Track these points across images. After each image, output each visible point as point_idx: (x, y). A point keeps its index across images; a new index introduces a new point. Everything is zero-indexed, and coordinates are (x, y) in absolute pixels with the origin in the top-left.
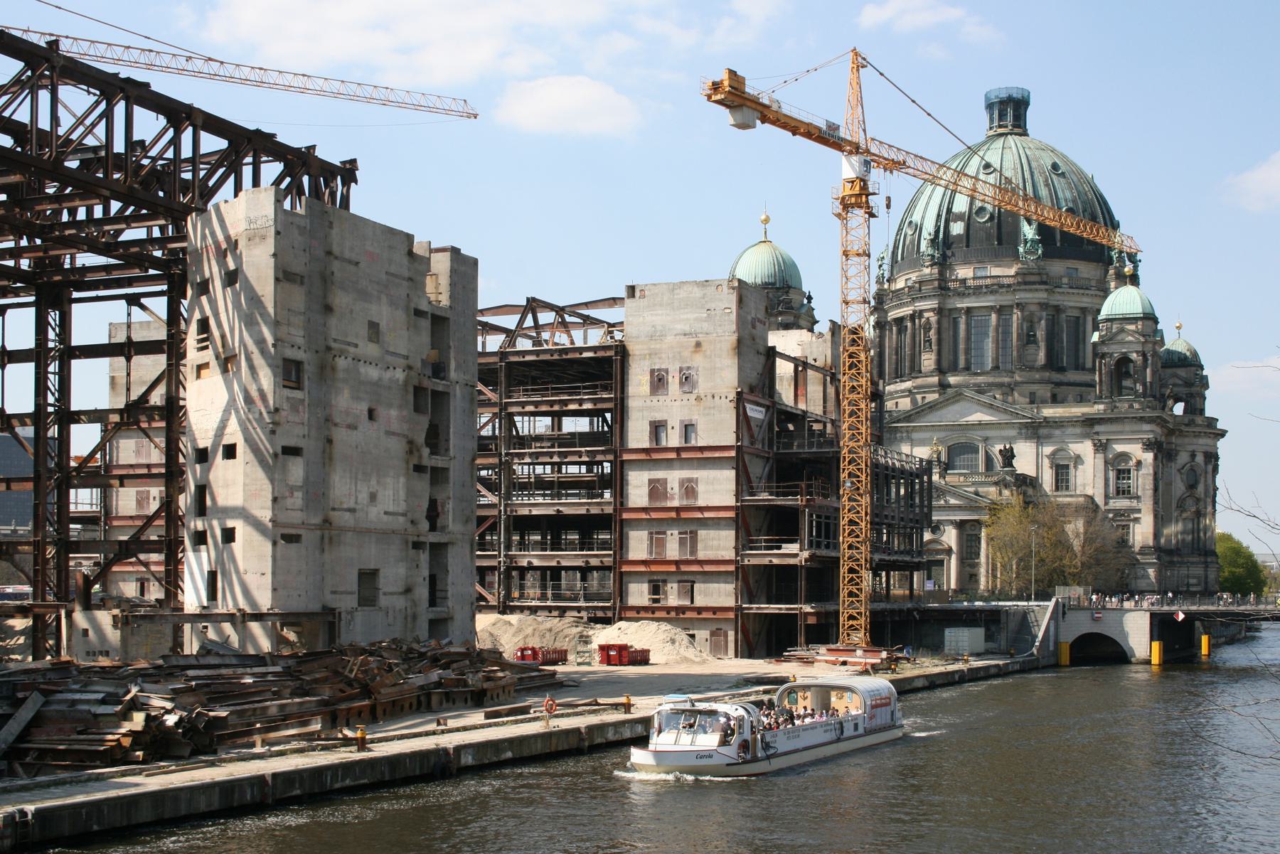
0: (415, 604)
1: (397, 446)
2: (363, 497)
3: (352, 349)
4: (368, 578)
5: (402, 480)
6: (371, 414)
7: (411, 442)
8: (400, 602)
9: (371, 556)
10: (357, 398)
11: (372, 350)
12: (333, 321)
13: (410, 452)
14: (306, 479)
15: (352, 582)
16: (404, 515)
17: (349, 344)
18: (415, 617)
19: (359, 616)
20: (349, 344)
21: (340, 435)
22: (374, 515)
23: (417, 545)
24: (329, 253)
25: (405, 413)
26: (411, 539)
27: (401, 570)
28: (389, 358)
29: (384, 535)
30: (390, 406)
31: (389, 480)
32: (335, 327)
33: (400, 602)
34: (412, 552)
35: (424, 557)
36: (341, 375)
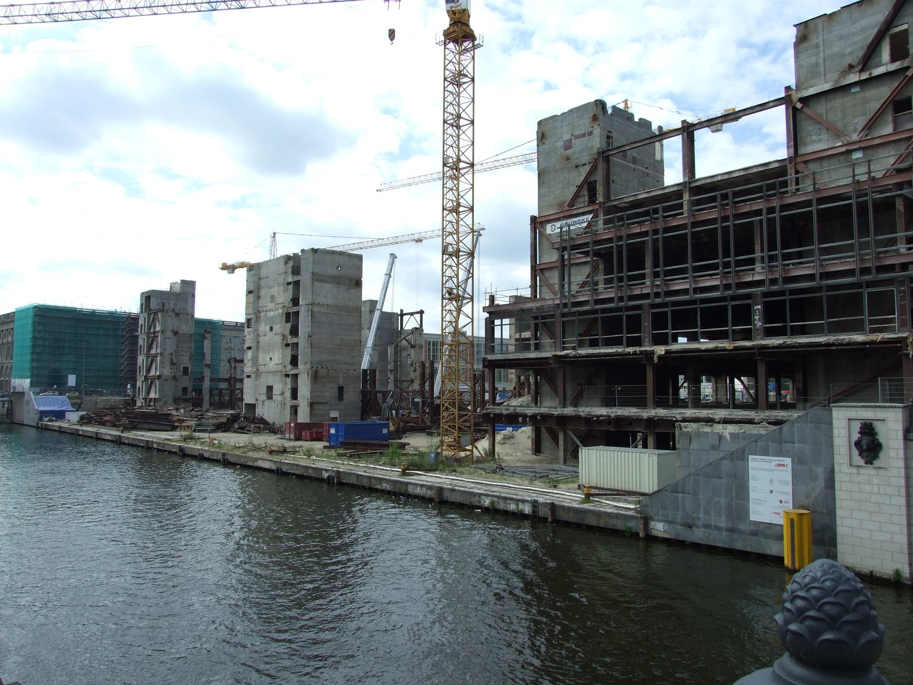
0: (285, 399)
1: (279, 339)
2: (268, 359)
3: (265, 308)
4: (270, 389)
5: (280, 351)
6: (271, 329)
7: (284, 336)
8: (279, 398)
9: (270, 380)
10: (266, 325)
11: (271, 306)
12: (260, 300)
13: (283, 339)
14: (252, 357)
15: (264, 390)
16: (281, 364)
17: (265, 306)
18: (285, 404)
19: (266, 403)
20: (265, 306)
21: (262, 339)
22: (272, 366)
23: (287, 376)
24: (260, 279)
25: (282, 325)
26: (284, 373)
27: (280, 386)
28: (277, 306)
29: (274, 373)
30: (277, 324)
31: (276, 352)
32: (262, 303)
33: (279, 398)
34: (284, 378)
35: (289, 380)
36: (262, 318)
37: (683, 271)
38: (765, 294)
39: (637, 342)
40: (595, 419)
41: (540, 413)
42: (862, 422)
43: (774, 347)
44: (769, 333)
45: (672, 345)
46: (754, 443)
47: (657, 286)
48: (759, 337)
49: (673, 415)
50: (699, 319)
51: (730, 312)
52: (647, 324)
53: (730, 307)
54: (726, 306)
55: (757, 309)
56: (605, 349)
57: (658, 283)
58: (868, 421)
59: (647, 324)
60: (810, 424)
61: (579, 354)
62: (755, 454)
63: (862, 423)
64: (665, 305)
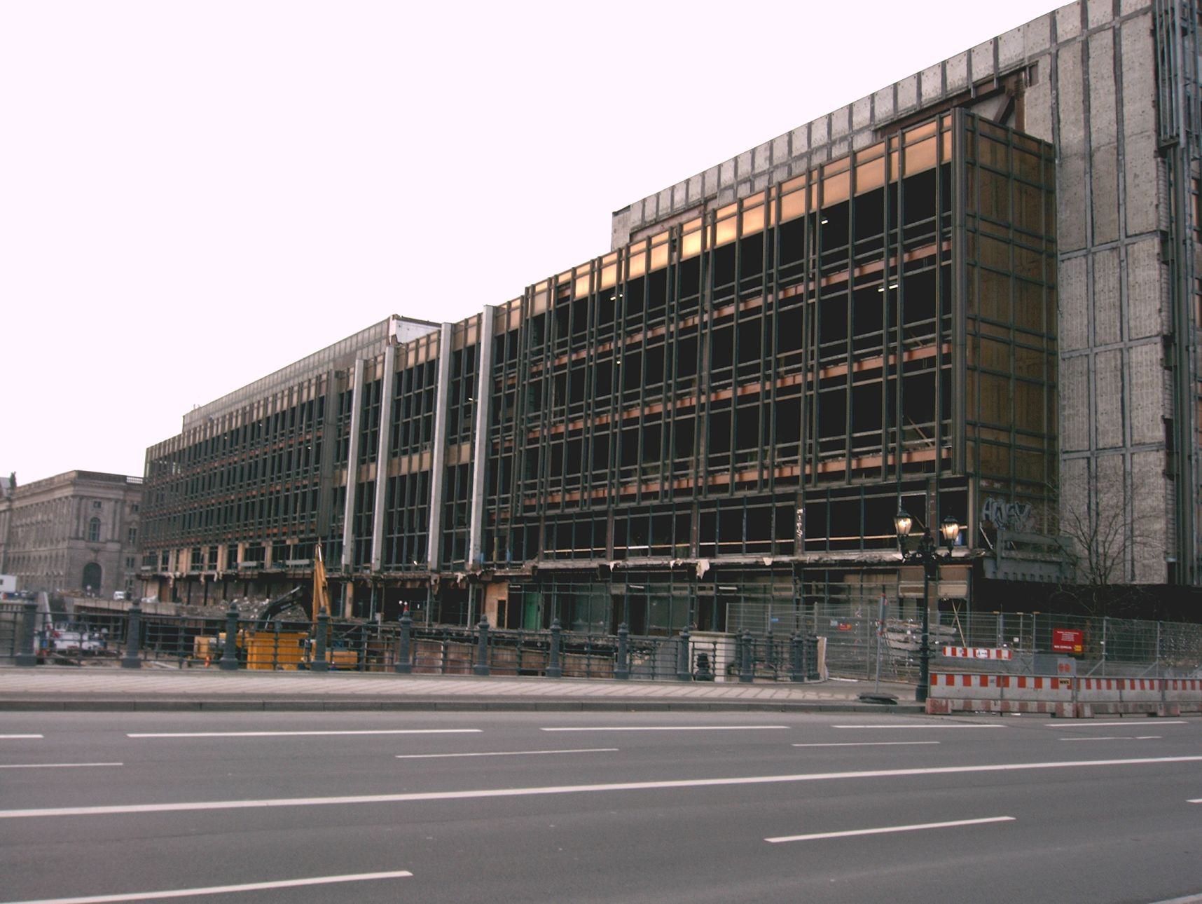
43: (811, 565)
44: (810, 547)
55: (800, 514)
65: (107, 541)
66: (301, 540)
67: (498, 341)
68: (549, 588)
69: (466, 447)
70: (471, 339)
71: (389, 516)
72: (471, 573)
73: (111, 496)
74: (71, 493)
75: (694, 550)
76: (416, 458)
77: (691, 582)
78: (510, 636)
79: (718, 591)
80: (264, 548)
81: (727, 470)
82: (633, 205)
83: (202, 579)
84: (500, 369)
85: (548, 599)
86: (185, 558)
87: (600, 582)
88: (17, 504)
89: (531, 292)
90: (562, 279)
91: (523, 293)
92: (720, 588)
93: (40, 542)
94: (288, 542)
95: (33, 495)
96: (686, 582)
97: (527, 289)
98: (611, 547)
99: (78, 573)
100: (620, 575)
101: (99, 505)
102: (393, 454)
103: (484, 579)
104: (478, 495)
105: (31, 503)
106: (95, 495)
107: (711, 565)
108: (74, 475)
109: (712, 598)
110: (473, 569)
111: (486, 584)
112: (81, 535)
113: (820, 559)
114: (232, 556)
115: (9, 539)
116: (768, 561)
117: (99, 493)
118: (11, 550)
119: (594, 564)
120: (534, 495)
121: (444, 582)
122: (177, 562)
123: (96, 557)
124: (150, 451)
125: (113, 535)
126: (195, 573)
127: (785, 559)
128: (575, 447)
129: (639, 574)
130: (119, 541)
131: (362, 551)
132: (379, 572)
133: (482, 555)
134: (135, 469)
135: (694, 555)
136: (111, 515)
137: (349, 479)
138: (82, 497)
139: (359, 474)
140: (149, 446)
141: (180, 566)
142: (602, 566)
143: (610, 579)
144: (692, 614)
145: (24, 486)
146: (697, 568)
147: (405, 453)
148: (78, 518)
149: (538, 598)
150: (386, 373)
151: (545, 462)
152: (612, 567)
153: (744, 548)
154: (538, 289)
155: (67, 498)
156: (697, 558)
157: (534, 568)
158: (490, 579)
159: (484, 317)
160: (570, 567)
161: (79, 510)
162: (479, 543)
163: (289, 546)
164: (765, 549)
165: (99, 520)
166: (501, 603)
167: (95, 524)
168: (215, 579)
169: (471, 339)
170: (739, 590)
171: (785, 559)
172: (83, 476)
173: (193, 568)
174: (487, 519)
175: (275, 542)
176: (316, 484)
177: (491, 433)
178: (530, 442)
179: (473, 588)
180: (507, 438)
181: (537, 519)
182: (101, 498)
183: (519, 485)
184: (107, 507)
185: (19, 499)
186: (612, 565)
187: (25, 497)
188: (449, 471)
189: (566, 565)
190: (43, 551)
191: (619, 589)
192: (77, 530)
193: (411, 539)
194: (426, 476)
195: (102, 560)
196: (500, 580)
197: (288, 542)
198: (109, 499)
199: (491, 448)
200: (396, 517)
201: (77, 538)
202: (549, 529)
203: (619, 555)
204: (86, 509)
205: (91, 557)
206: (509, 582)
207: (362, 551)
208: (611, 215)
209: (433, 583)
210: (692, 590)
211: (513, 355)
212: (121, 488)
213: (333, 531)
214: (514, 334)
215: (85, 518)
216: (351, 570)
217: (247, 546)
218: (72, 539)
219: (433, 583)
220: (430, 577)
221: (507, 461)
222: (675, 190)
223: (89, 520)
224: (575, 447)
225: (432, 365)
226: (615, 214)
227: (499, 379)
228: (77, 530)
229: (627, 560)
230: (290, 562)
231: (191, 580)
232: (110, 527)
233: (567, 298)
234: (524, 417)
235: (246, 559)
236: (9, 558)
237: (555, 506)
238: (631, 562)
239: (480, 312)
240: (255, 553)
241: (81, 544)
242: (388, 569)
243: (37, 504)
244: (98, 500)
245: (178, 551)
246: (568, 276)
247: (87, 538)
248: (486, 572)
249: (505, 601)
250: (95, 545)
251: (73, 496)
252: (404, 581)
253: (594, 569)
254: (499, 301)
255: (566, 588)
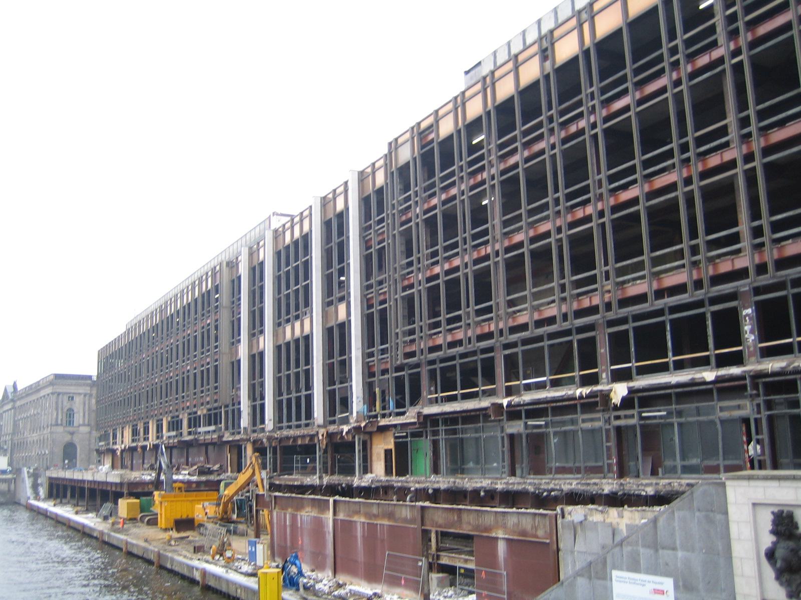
37: (640, 266)
38: (757, 291)
39: (592, 380)
40: (545, 494)
41: (483, 487)
42: (776, 510)
43: (775, 374)
44: (768, 353)
45: (637, 380)
46: (617, 549)
47: (609, 291)
48: (753, 359)
49: (643, 488)
50: (669, 337)
51: (709, 323)
52: (603, 350)
53: (709, 316)
54: (703, 315)
55: (747, 315)
56: (555, 391)
57: (609, 287)
58: (786, 509)
59: (603, 350)
60: (697, 514)
61: (524, 401)
62: (621, 569)
63: (773, 513)
64: (623, 321)
65: (79, 426)
66: (209, 410)
67: (365, 201)
68: (435, 433)
69: (342, 308)
70: (340, 206)
71: (278, 381)
72: (355, 425)
73: (81, 391)
74: (51, 391)
75: (604, 375)
76: (297, 324)
77: (603, 411)
78: (399, 484)
79: (642, 418)
80: (181, 420)
81: (643, 277)
82: (483, 60)
83: (139, 449)
84: (370, 227)
85: (435, 444)
86: (128, 433)
87: (494, 421)
88: (18, 403)
89: (394, 146)
90: (424, 125)
91: (386, 151)
92: (644, 415)
93: (33, 430)
94: (199, 413)
95: (28, 395)
96: (598, 411)
97: (390, 144)
98: (501, 383)
99: (59, 451)
100: (514, 413)
101: (73, 398)
102: (278, 325)
103: (369, 429)
104: (357, 349)
105: (26, 402)
106: (69, 391)
107: (631, 391)
108: (52, 377)
109: (634, 427)
110: (357, 421)
111: (371, 434)
112: (59, 422)
113: (788, 365)
114: (159, 428)
115: (14, 430)
116: (709, 375)
117: (72, 389)
118: (16, 438)
119: (485, 403)
120: (413, 341)
121: (330, 436)
122: (122, 437)
123: (72, 438)
124: (101, 353)
125: (84, 421)
126: (134, 444)
127: (735, 370)
128: (453, 286)
129: (535, 411)
130: (89, 425)
131: (258, 413)
132: (273, 431)
133: (365, 406)
134: (90, 368)
135: (605, 381)
136: (82, 407)
137: (243, 352)
138: (59, 394)
139: (250, 346)
140: (99, 348)
141: (124, 440)
142: (493, 404)
143: (505, 417)
144: (608, 448)
145: (22, 390)
146: (612, 395)
147: (288, 321)
148: (57, 409)
149: (425, 445)
150: (267, 255)
151: (422, 305)
152: (505, 405)
153: (671, 366)
154: (400, 141)
155: (48, 395)
156: (608, 384)
157: (419, 414)
158: (375, 429)
159: (349, 184)
160: (458, 409)
161: (57, 403)
162: (361, 395)
163: (200, 417)
164: (704, 362)
165: (73, 411)
166: (388, 453)
167: (70, 414)
168: (148, 449)
169: (340, 206)
170: (670, 414)
171: (735, 370)
172: (58, 377)
173: (133, 441)
174: (369, 372)
175: (190, 414)
176: (216, 361)
177: (366, 288)
178: (404, 289)
179: (359, 439)
180: (380, 292)
181: (418, 365)
182: (74, 393)
183: (397, 334)
184: (78, 399)
185: (19, 399)
186: (505, 402)
187: (22, 398)
188: (329, 333)
189: (452, 407)
190: (35, 436)
191: (516, 427)
192: (57, 419)
193: (298, 399)
194: (308, 339)
195: (76, 440)
196: (383, 429)
197: (199, 413)
198: (80, 394)
199: (367, 303)
200: (284, 381)
201: (57, 425)
202: (432, 374)
203: (509, 392)
204: (62, 402)
205: (68, 438)
206: (394, 430)
207: (258, 413)
208: (463, 74)
209: (321, 437)
210: (608, 421)
211: (380, 210)
212: (87, 385)
213: (233, 399)
214: (380, 192)
215: (62, 410)
216: (249, 430)
217: (169, 419)
218: (54, 426)
219: (321, 437)
220: (318, 433)
221: (383, 312)
222: (526, 34)
223: (65, 410)
224: (453, 286)
225: (306, 239)
226: (467, 73)
227: (368, 237)
228: (57, 419)
229: (521, 396)
230: (202, 429)
231: (132, 450)
232: (82, 414)
233: (432, 141)
234: (397, 265)
235: (169, 430)
236: (15, 444)
237: (438, 348)
238: (527, 397)
239: (346, 180)
240: (175, 425)
241: (60, 429)
242: (281, 428)
243: (31, 402)
244: (71, 395)
245: (123, 428)
246: (431, 120)
247: (64, 424)
248: (370, 422)
249: (391, 450)
250: (70, 429)
251: (53, 394)
252: (295, 439)
253: (486, 409)
254: (363, 164)
255: (454, 432)
